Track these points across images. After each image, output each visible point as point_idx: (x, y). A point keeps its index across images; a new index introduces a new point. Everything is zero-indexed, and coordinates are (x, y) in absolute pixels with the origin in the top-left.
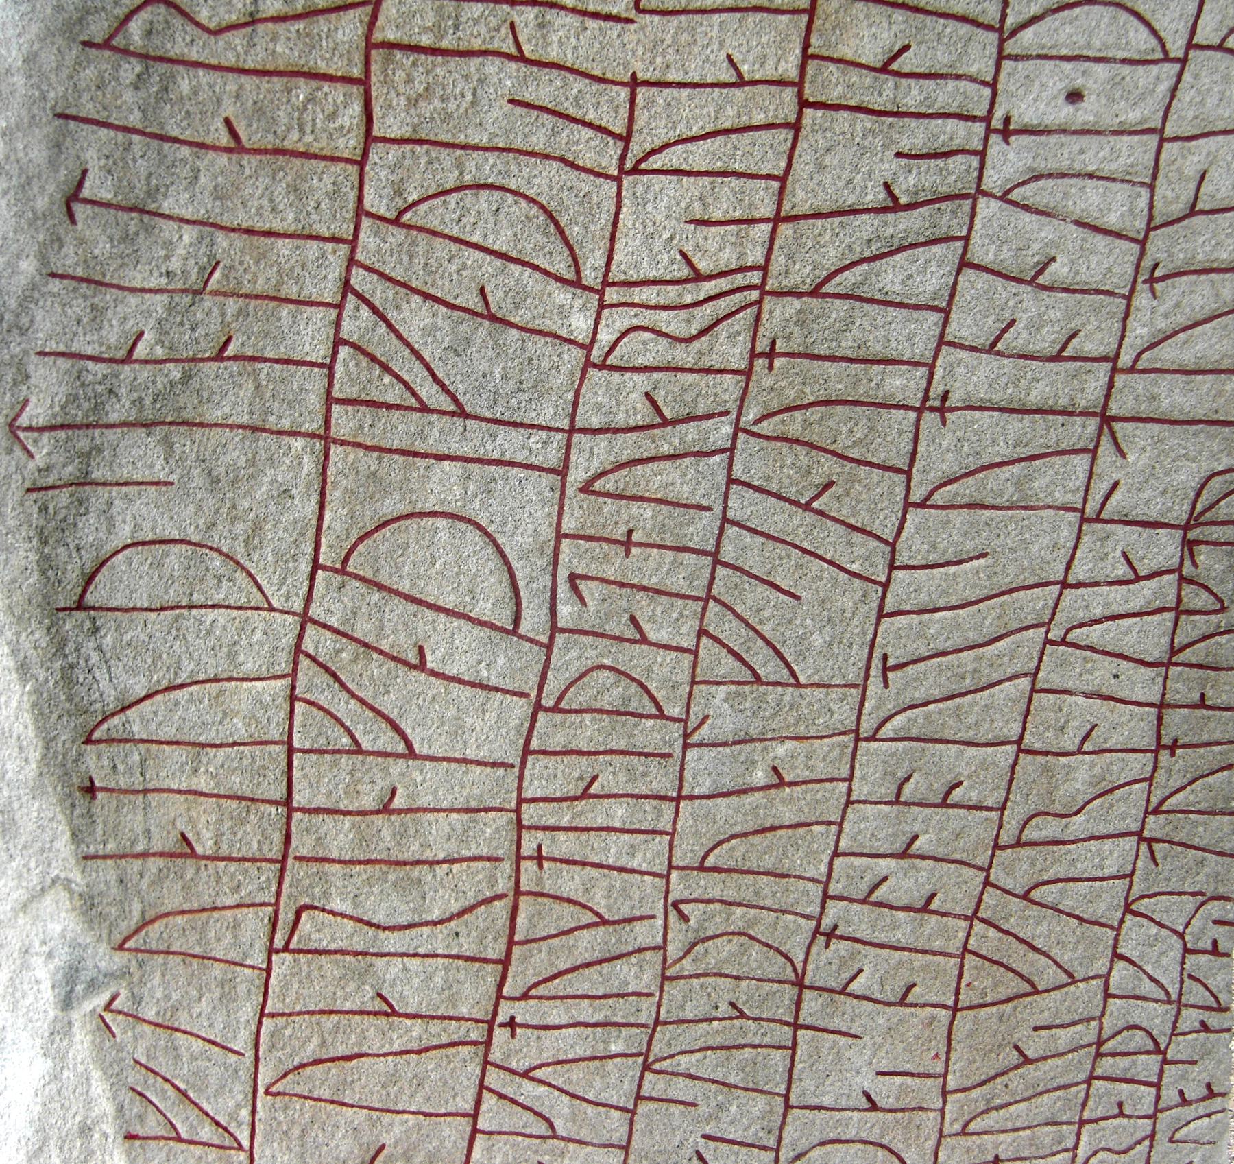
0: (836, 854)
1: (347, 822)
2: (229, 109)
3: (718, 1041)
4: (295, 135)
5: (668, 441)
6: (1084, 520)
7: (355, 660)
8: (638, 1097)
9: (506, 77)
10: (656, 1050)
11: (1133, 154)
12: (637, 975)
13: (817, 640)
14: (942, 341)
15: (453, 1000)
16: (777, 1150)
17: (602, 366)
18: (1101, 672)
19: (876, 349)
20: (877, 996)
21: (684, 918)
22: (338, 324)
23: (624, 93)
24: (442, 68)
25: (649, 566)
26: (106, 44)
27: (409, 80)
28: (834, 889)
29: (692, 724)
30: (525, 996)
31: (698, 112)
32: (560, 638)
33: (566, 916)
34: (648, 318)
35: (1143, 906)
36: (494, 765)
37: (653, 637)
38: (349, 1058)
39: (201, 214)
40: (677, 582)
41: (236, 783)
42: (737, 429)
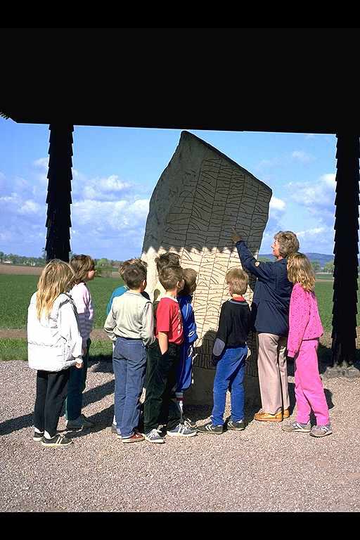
12: (205, 310)
25: (206, 273)
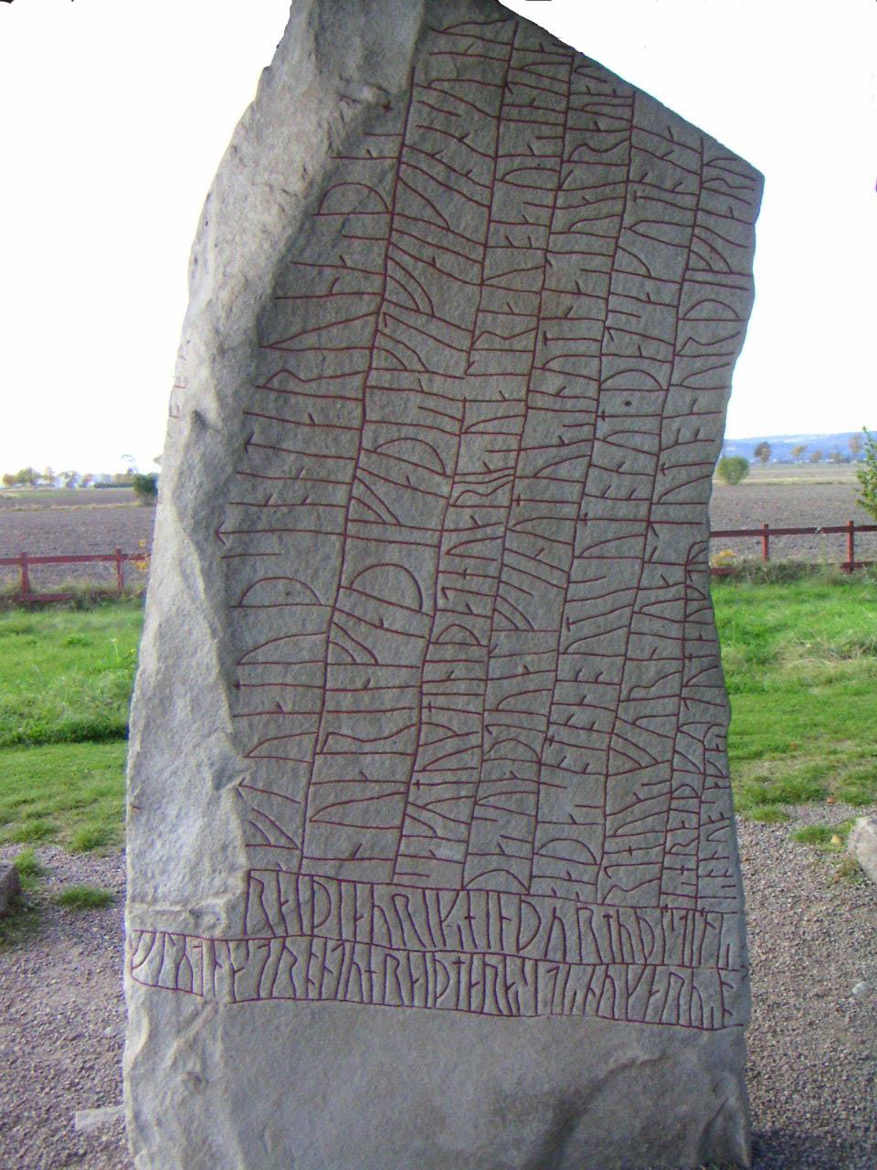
0: (552, 704)
1: (349, 694)
2: (311, 410)
3: (504, 790)
4: (336, 420)
5: (480, 534)
6: (644, 562)
7: (354, 625)
8: (473, 818)
9: (416, 399)
10: (480, 793)
11: (650, 424)
12: (472, 759)
13: (540, 612)
14: (583, 494)
15: (393, 773)
16: (533, 843)
17: (454, 506)
18: (657, 625)
19: (558, 498)
20: (573, 769)
21: (490, 733)
22: (351, 491)
23: (461, 405)
24: (393, 395)
25: (474, 584)
26: (264, 387)
27: (380, 400)
28: (553, 719)
29: (491, 647)
30: (424, 770)
31: (487, 411)
32: (438, 613)
33: (441, 732)
34: (472, 487)
35: (685, 728)
36: (412, 667)
37: (475, 612)
38: (347, 803)
39: (298, 449)
40: (485, 589)
41: (303, 679)
42: (506, 529)
